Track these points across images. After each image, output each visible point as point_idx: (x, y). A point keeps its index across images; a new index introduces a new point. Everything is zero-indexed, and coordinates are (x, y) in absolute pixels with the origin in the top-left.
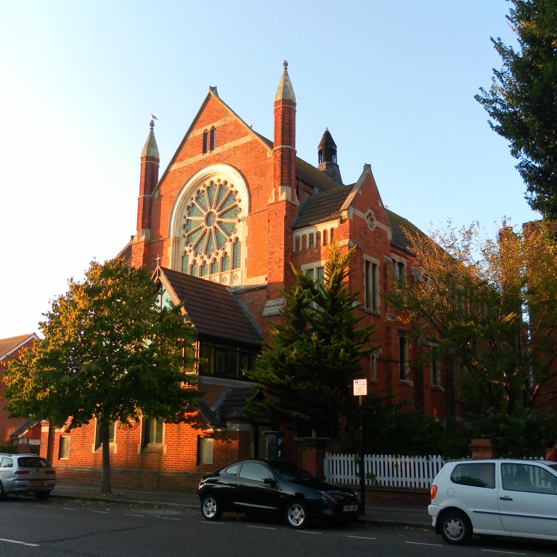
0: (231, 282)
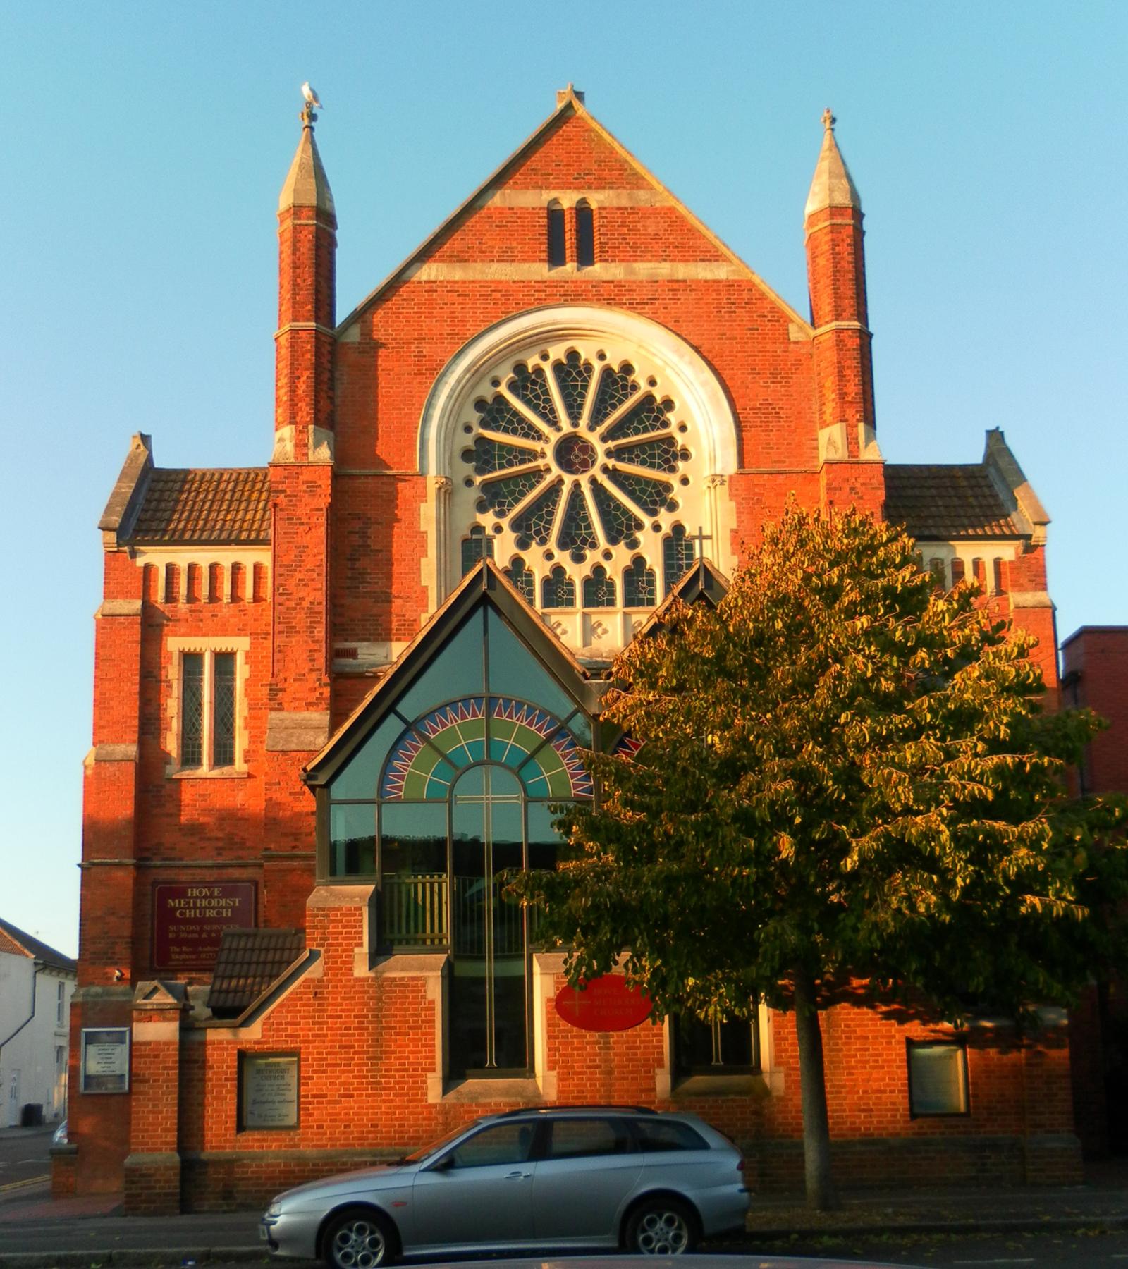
0: (586, 643)
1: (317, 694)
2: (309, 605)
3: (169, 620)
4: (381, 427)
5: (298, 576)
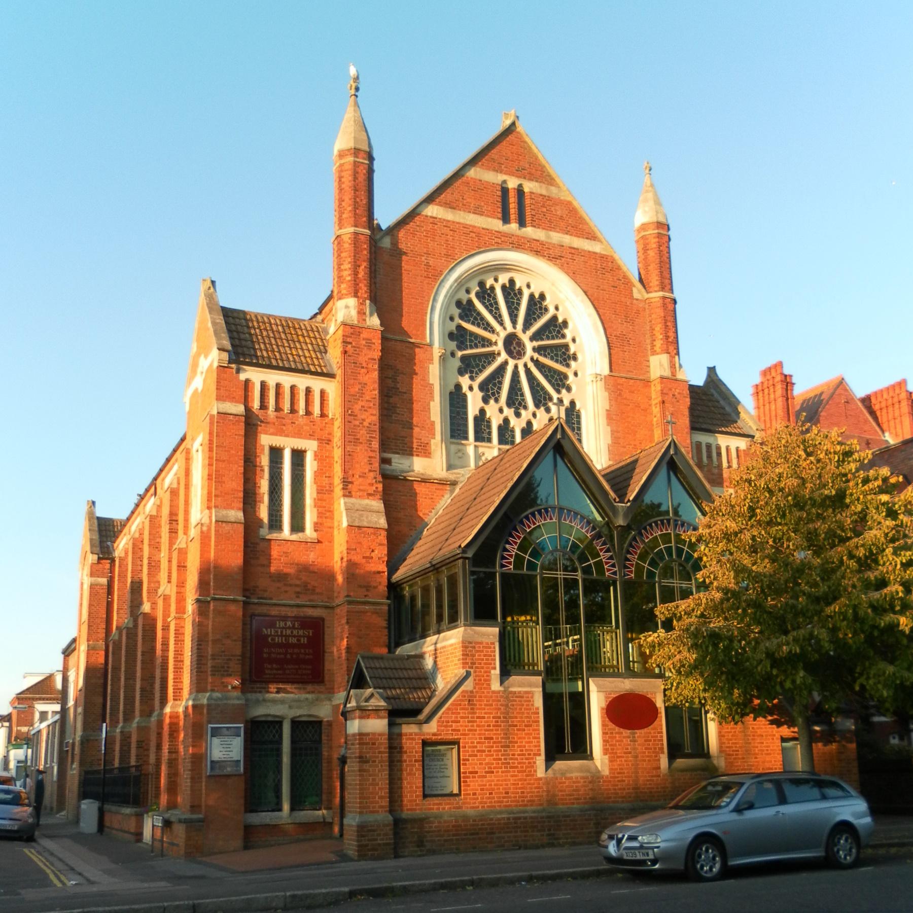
1: (374, 488)
2: (368, 425)
3: (262, 422)
4: (405, 309)
5: (360, 403)
